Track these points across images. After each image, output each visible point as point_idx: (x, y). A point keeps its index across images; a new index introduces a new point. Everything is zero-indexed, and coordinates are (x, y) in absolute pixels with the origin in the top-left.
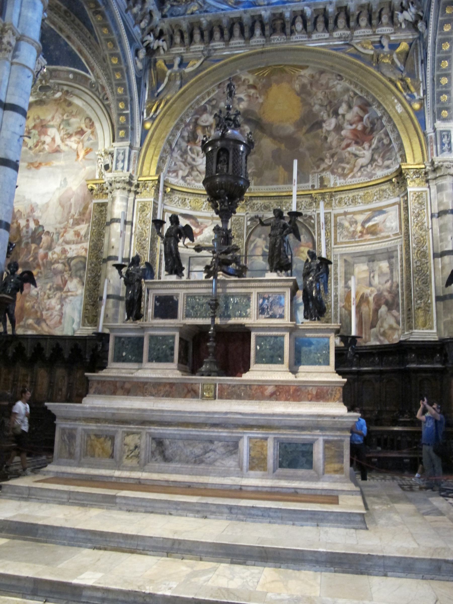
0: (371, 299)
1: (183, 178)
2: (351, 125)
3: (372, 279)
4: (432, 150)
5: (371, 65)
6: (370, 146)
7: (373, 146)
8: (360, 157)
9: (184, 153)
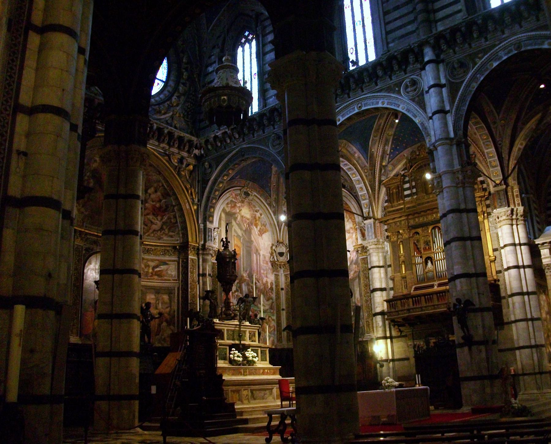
2: (153, 202)
3: (157, 305)
4: (202, 236)
6: (162, 219)
7: (164, 220)
8: (154, 224)
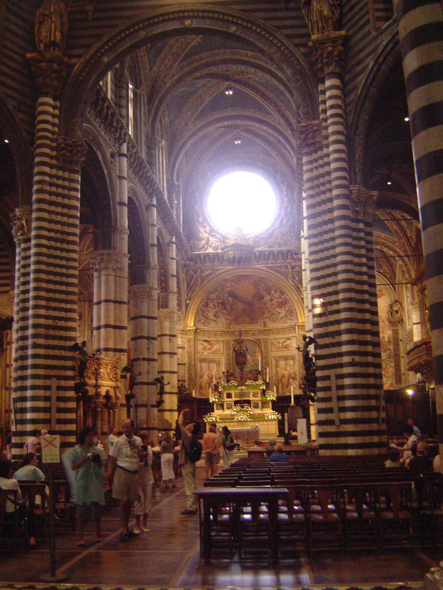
0: (286, 376)
1: (203, 324)
5: (284, 276)
9: (203, 312)
